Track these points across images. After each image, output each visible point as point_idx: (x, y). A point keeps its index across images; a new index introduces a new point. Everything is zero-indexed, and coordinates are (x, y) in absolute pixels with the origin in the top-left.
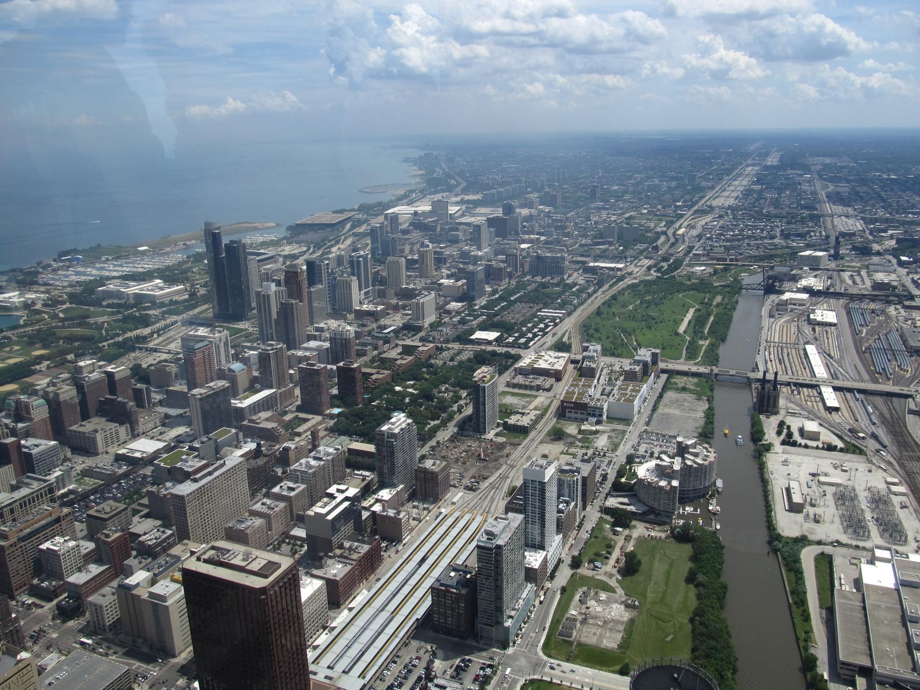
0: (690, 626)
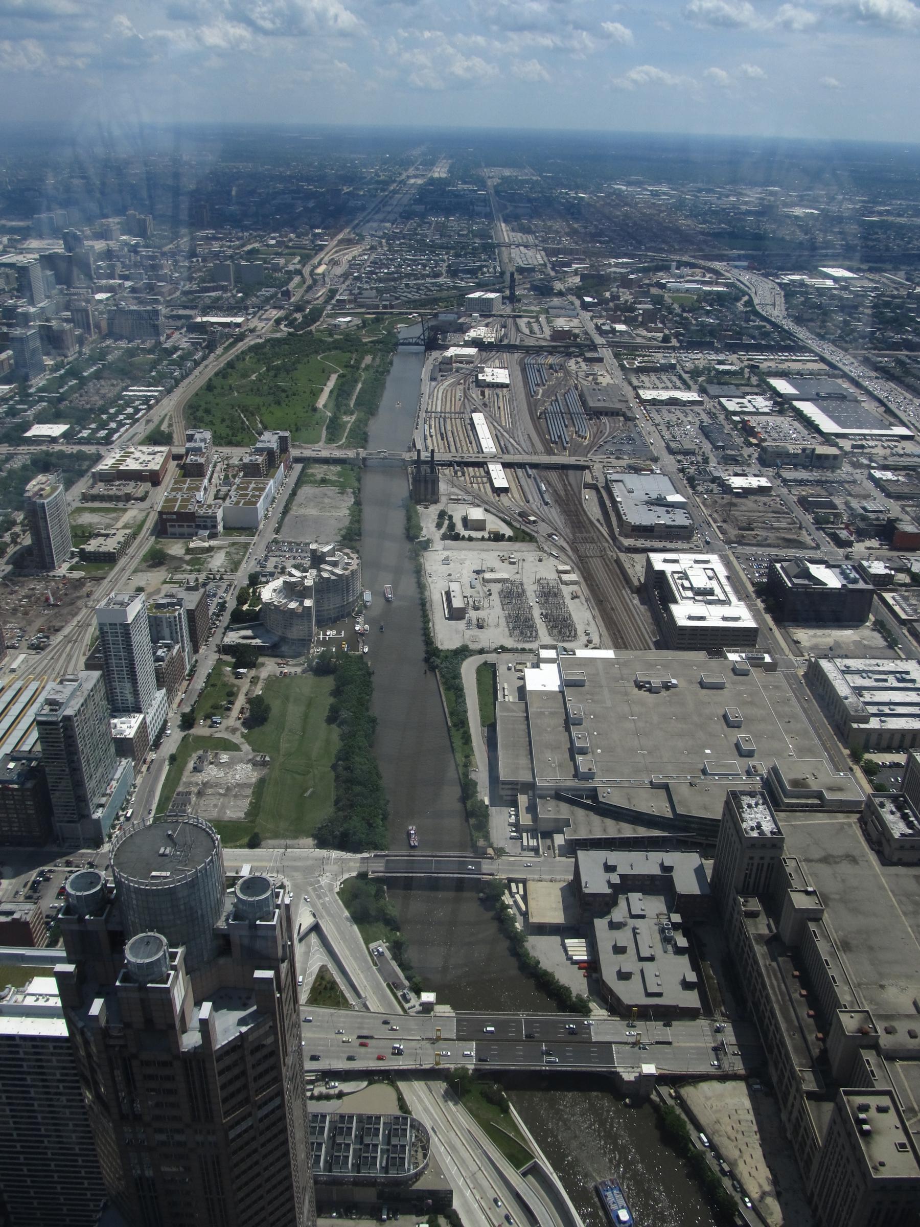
0: (333, 774)
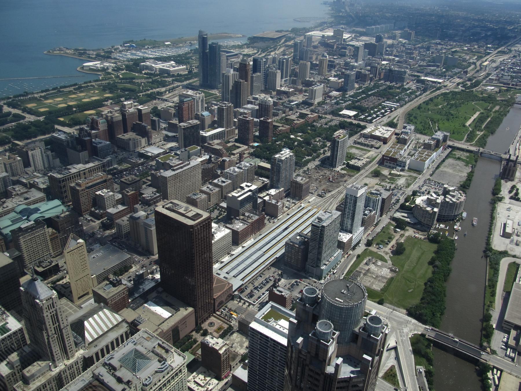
0: (424, 287)
